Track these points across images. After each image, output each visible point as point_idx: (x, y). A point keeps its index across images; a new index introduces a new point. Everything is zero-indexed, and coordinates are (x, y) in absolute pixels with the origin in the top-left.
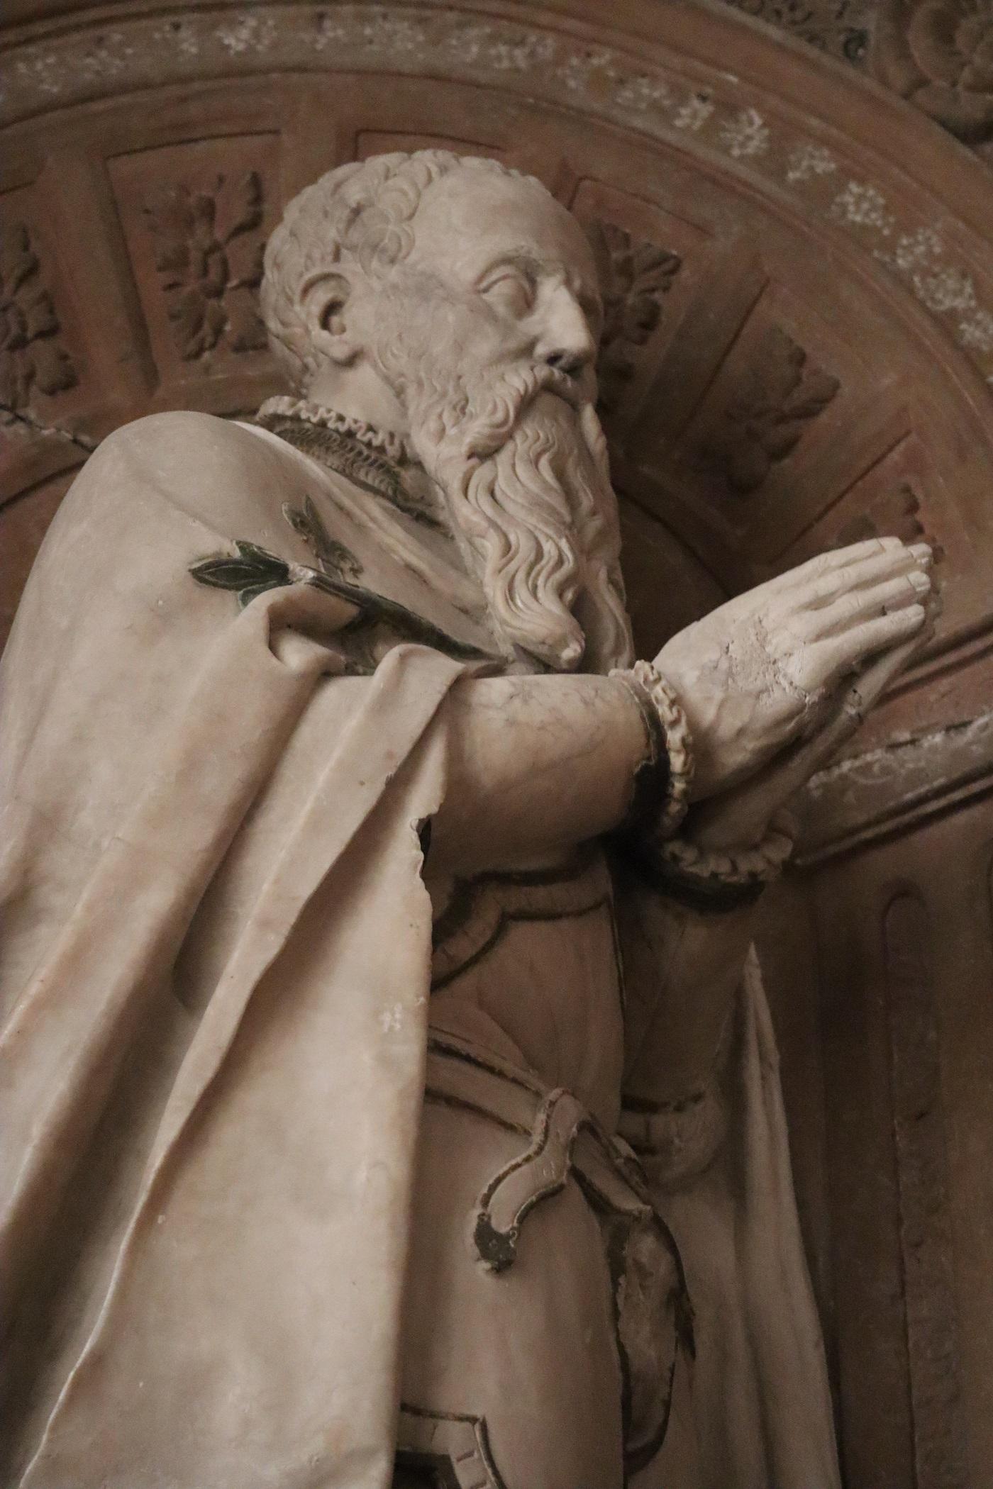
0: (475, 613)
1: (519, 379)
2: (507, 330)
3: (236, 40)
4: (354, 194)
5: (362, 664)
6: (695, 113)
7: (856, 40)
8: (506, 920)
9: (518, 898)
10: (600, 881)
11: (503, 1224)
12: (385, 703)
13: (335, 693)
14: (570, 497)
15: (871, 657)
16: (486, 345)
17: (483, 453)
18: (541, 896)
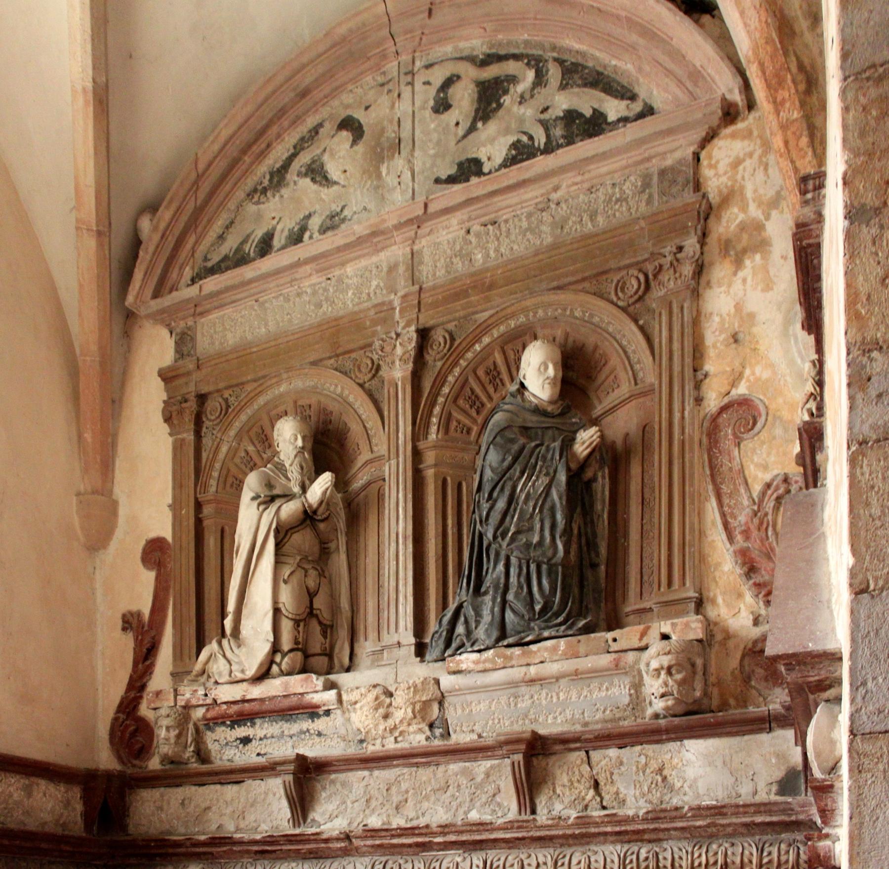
1: (295, 453)
2: (293, 444)
3: (282, 390)
6: (333, 387)
8: (292, 534)
9: (293, 531)
10: (308, 522)
11: (286, 577)
14: (302, 468)
15: (327, 489)
16: (291, 447)
18: (296, 529)
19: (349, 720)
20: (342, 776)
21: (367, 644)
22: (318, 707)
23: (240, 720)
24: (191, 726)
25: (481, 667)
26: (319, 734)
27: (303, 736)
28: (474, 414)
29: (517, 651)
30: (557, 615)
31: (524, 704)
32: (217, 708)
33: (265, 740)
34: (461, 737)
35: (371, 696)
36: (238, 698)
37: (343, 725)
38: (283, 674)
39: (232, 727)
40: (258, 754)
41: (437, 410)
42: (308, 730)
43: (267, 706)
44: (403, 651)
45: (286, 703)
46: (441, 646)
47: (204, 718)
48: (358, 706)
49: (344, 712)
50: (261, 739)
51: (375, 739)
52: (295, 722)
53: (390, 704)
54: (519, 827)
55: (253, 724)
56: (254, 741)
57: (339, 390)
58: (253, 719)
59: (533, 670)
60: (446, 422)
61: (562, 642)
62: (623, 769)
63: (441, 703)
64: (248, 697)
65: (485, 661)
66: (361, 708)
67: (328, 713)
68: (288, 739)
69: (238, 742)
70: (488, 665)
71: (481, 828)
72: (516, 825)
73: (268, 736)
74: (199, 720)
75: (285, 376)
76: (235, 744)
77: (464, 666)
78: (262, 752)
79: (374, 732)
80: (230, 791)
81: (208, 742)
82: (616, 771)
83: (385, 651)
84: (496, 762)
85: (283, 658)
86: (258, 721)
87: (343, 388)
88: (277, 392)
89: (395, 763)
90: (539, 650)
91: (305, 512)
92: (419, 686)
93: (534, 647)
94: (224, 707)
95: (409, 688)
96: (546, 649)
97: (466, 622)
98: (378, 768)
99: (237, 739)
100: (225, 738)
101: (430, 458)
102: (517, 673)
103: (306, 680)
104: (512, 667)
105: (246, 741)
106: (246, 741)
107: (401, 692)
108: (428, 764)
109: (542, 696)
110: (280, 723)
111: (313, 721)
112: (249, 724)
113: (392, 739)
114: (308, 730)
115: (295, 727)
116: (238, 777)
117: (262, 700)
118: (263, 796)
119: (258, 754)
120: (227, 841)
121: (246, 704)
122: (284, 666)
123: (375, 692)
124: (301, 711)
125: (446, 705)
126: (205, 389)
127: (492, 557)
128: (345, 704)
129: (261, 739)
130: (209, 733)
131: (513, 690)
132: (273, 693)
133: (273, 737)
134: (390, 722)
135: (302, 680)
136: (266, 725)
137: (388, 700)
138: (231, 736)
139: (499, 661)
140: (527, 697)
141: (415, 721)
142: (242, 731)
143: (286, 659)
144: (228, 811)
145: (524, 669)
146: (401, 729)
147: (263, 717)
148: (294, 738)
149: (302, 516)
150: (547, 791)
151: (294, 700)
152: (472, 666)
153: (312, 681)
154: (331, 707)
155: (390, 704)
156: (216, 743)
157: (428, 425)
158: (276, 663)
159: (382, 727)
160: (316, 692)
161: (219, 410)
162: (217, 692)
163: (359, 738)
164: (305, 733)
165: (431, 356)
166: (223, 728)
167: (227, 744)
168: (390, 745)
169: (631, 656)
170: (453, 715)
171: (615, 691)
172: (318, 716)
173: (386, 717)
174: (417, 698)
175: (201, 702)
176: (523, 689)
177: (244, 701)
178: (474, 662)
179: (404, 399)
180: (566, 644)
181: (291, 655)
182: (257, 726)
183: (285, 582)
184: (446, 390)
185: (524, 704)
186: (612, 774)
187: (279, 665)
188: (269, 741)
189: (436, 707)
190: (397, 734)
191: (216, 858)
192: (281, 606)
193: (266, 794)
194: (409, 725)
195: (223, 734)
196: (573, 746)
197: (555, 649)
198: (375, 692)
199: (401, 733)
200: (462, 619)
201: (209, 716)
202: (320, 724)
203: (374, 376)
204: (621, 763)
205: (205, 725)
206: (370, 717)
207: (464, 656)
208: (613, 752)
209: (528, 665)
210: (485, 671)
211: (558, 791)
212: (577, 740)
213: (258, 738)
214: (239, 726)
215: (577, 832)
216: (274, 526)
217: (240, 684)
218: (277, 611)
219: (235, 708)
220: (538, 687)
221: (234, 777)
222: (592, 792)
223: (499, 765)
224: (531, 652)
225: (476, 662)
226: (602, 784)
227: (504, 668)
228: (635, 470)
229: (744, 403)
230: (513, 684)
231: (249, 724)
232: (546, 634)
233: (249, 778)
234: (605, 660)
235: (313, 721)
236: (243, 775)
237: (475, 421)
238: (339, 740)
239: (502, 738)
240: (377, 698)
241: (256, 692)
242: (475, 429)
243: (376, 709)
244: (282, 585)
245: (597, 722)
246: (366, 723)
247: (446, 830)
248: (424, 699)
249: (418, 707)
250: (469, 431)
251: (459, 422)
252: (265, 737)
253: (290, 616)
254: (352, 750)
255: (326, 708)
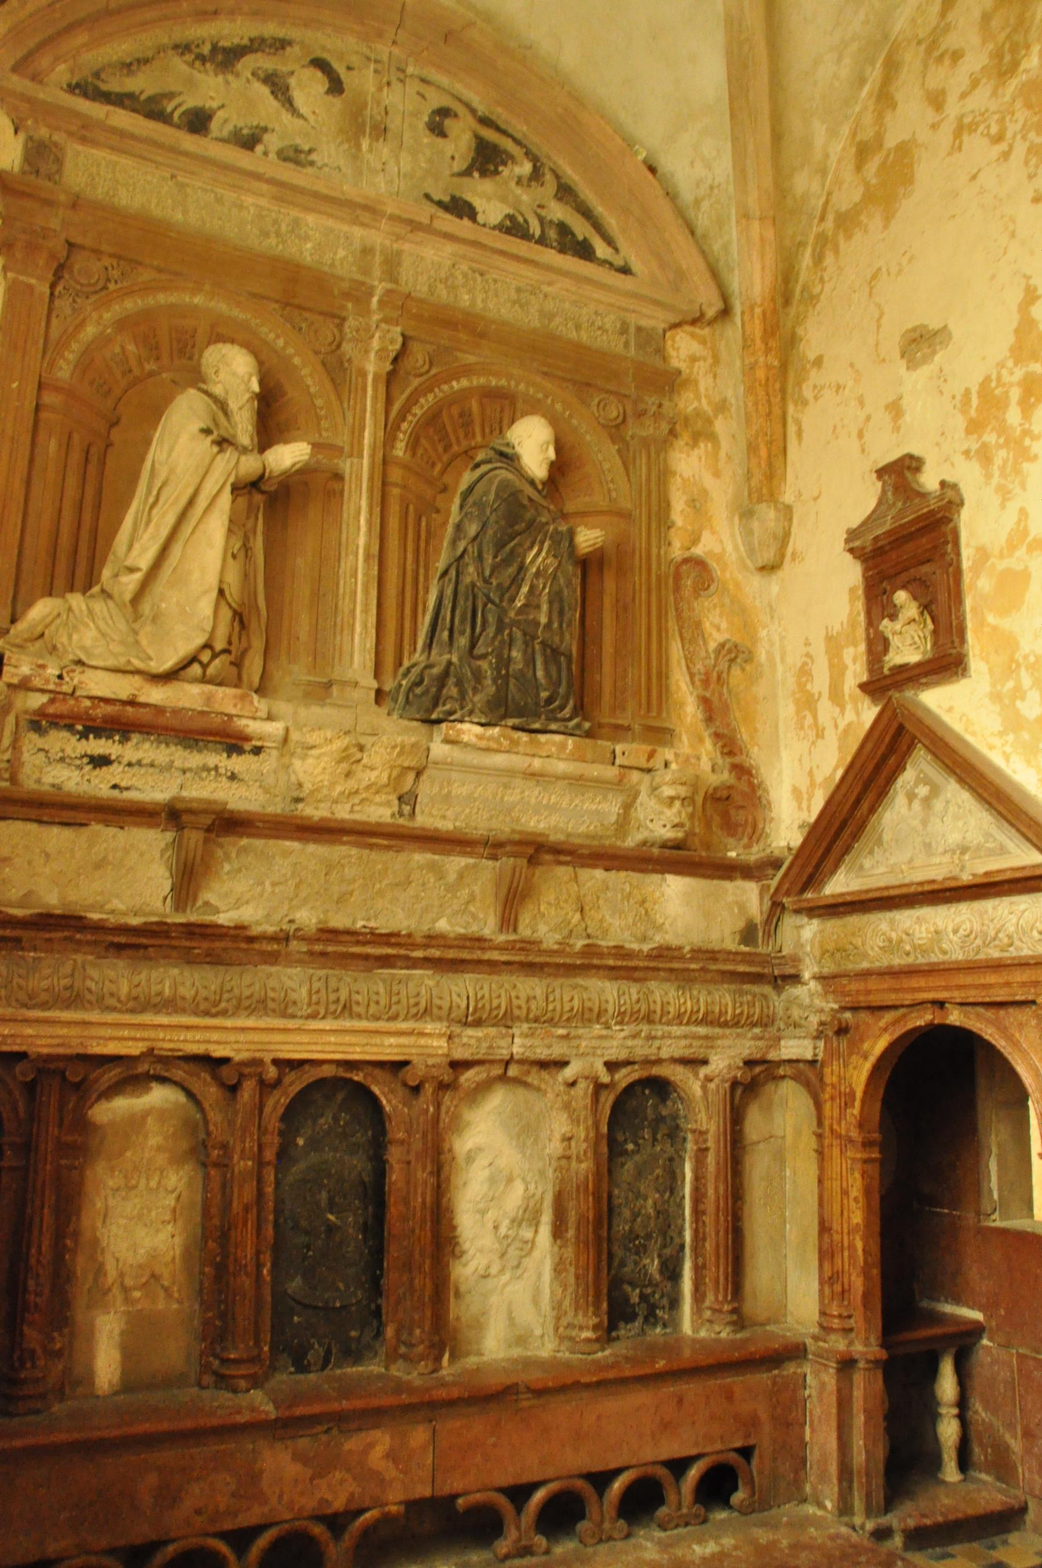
0: (234, 436)
1: (247, 396)
4: (224, 351)
5: (221, 451)
6: (272, 336)
7: (300, 329)
12: (228, 461)
13: (219, 457)
16: (243, 387)
17: (240, 408)
19: (287, 767)
20: (258, 843)
21: (295, 668)
22: (247, 739)
23: (104, 729)
24: (11, 719)
25: (483, 744)
26: (233, 777)
27: (204, 774)
28: (440, 449)
29: (524, 737)
30: (562, 708)
31: (512, 797)
32: (72, 702)
33: (136, 768)
34: (426, 819)
35: (339, 744)
36: (124, 695)
37: (275, 772)
38: (204, 680)
39: (84, 735)
40: (115, 787)
41: (404, 426)
42: (216, 768)
43: (167, 719)
44: (356, 694)
45: (199, 723)
46: (427, 701)
47: (41, 712)
48: (314, 752)
49: (282, 755)
50: (130, 765)
51: (320, 801)
52: (200, 751)
53: (359, 761)
54: (522, 949)
55: (125, 739)
56: (115, 765)
57: (281, 342)
58: (129, 732)
59: (537, 763)
60: (414, 445)
61: (570, 741)
62: (609, 894)
63: (419, 774)
64: (142, 699)
65: (489, 739)
66: (318, 757)
67: (257, 751)
68: (177, 773)
69: (85, 760)
70: (494, 746)
71: (477, 944)
72: (518, 946)
73: (145, 762)
74: (26, 712)
75: (207, 287)
76: (78, 762)
77: (465, 738)
78: (123, 784)
79: (325, 792)
80: (56, 837)
81: (25, 749)
82: (602, 896)
83: (334, 687)
84: (471, 861)
85: (215, 656)
86: (135, 738)
87: (286, 343)
88: (187, 299)
89: (345, 838)
90: (546, 743)
91: (262, 477)
92: (408, 748)
93: (543, 738)
94: (88, 703)
95: (394, 747)
96: (554, 744)
97: (459, 683)
98: (315, 841)
99: (86, 755)
100: (63, 751)
101: (396, 475)
102: (518, 761)
103: (243, 697)
104: (517, 753)
105: (101, 761)
106: (101, 761)
107: (382, 750)
108: (388, 848)
109: (533, 793)
110: (173, 748)
111: (229, 757)
112: (117, 738)
113: (348, 807)
114: (216, 768)
115: (195, 759)
116: (81, 817)
117: (159, 710)
118: (119, 854)
119: (115, 787)
120: (72, 923)
121: (129, 709)
122: (211, 670)
123: (346, 740)
124: (218, 739)
125: (424, 777)
126: (78, 240)
127: (491, 619)
128: (291, 745)
129: (130, 765)
130: (33, 736)
131: (505, 780)
132: (185, 703)
133: (152, 765)
134: (352, 784)
135: (235, 697)
136: (147, 745)
137: (359, 755)
138: (74, 749)
139: (505, 743)
140: (518, 791)
141: (387, 789)
142: (98, 746)
143: (217, 662)
144: (47, 870)
145: (528, 759)
146: (364, 795)
147: (148, 733)
148: (188, 775)
149: (253, 478)
150: (531, 907)
151: (216, 721)
152: (474, 740)
153: (252, 702)
154: (266, 744)
155: (359, 761)
156: (42, 755)
157: (395, 438)
158: (201, 663)
159: (339, 789)
160: (254, 718)
161: (93, 281)
162: (84, 678)
163: (295, 794)
164: (209, 770)
165: (407, 364)
166: (65, 734)
167: (62, 760)
168: (343, 813)
169: (635, 776)
170: (426, 790)
171: (605, 807)
172: (240, 751)
173: (348, 775)
174: (399, 762)
175: (51, 687)
176: (518, 782)
177: (132, 703)
178: (477, 736)
179: (375, 398)
180: (574, 743)
181: (224, 657)
182: (130, 744)
183: (234, 556)
184: (417, 411)
185: (512, 797)
186: (598, 898)
187: (205, 666)
188: (143, 770)
189: (411, 777)
190: (357, 801)
191: (22, 949)
192: (225, 587)
193: (126, 852)
194: (377, 792)
195: (61, 741)
196: (563, 858)
197: (563, 746)
198: (346, 740)
199: (362, 801)
200: (452, 680)
201: (51, 710)
202: (238, 763)
203: (333, 352)
204: (607, 888)
205: (32, 722)
206: (329, 771)
207: (466, 726)
208: (599, 874)
209: (534, 755)
210: (488, 750)
211: (542, 908)
212: (571, 853)
213: (125, 761)
214: (98, 736)
215: (578, 962)
216: (232, 479)
217: (130, 676)
218: (221, 592)
219: (109, 709)
220: (533, 783)
221: (67, 815)
222: (578, 916)
223: (475, 866)
224: (539, 743)
225: (480, 737)
226: (587, 908)
227: (508, 752)
228: (610, 584)
229: (700, 563)
230: (511, 772)
231: (117, 738)
232: (553, 727)
233: (99, 822)
234: (611, 772)
235: (229, 757)
236: (92, 816)
237: (440, 458)
238: (260, 791)
239: (517, 837)
240: (346, 749)
241: (156, 695)
242: (438, 467)
243: (339, 762)
244: (230, 560)
245: (579, 836)
246: (319, 778)
247: (433, 942)
248: (406, 764)
249: (395, 773)
250: (433, 465)
251: (426, 450)
252: (139, 763)
253: (234, 605)
254: (277, 807)
255: (259, 744)
